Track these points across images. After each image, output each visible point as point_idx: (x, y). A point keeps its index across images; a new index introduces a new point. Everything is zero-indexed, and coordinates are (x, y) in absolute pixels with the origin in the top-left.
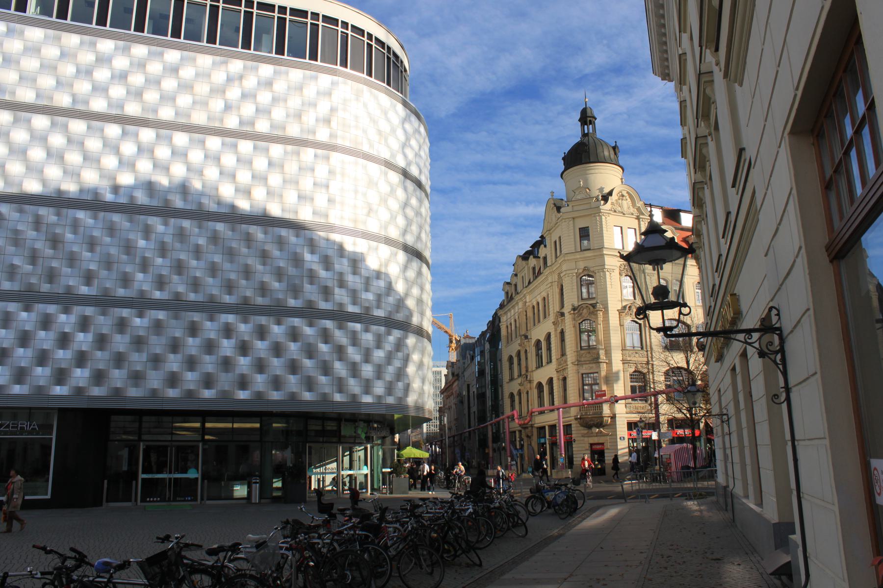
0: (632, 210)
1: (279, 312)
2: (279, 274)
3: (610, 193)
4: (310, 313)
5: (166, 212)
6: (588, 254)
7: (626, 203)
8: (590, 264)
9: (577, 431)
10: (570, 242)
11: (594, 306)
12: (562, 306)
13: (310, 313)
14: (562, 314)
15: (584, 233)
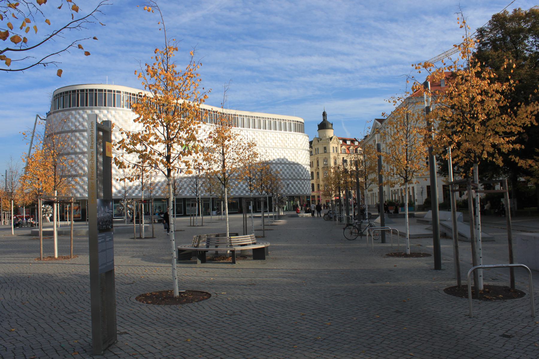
0: (337, 142)
1: (297, 179)
2: (296, 173)
3: (332, 137)
4: (300, 179)
5: (281, 163)
6: (326, 154)
7: (335, 141)
8: (326, 156)
9: (322, 197)
10: (321, 150)
11: (328, 167)
12: (318, 165)
13: (300, 179)
14: (318, 168)
15: (325, 148)
